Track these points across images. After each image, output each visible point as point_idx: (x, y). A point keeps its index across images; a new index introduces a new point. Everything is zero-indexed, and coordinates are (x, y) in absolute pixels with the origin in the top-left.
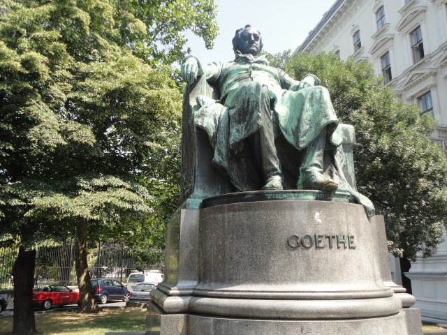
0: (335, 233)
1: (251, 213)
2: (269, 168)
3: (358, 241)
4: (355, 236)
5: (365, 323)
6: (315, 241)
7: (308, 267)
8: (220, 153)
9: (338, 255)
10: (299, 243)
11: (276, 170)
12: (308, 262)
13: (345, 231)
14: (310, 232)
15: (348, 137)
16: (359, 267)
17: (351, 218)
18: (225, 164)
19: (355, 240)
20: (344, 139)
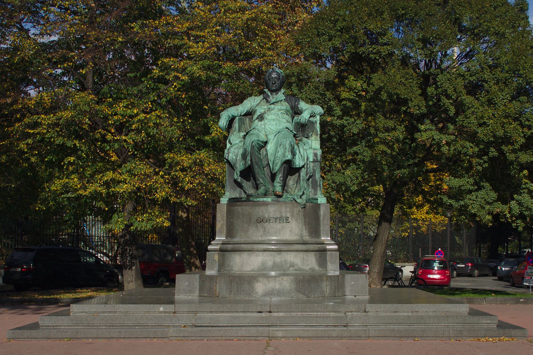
0: (279, 216)
1: (243, 207)
2: (258, 182)
3: (291, 219)
4: (290, 217)
5: (283, 253)
6: (268, 220)
7: (264, 231)
8: (237, 174)
9: (279, 226)
10: (261, 221)
11: (262, 183)
12: (265, 229)
13: (284, 215)
14: (266, 216)
15: (317, 157)
16: (290, 231)
17: (288, 209)
18: (239, 180)
19: (290, 219)
20: (314, 159)
